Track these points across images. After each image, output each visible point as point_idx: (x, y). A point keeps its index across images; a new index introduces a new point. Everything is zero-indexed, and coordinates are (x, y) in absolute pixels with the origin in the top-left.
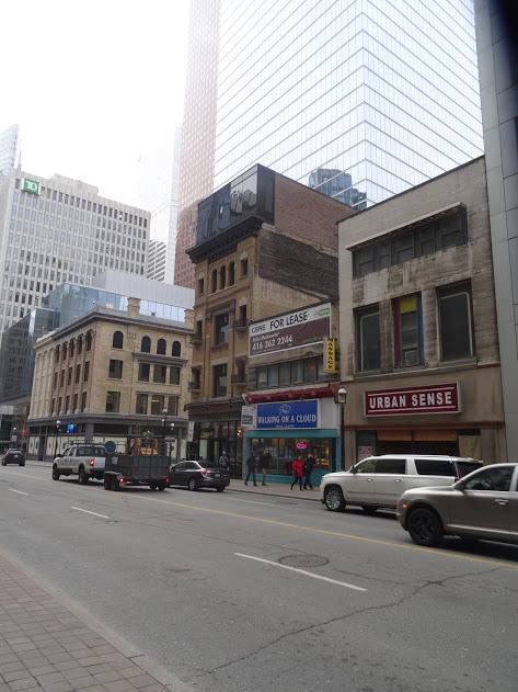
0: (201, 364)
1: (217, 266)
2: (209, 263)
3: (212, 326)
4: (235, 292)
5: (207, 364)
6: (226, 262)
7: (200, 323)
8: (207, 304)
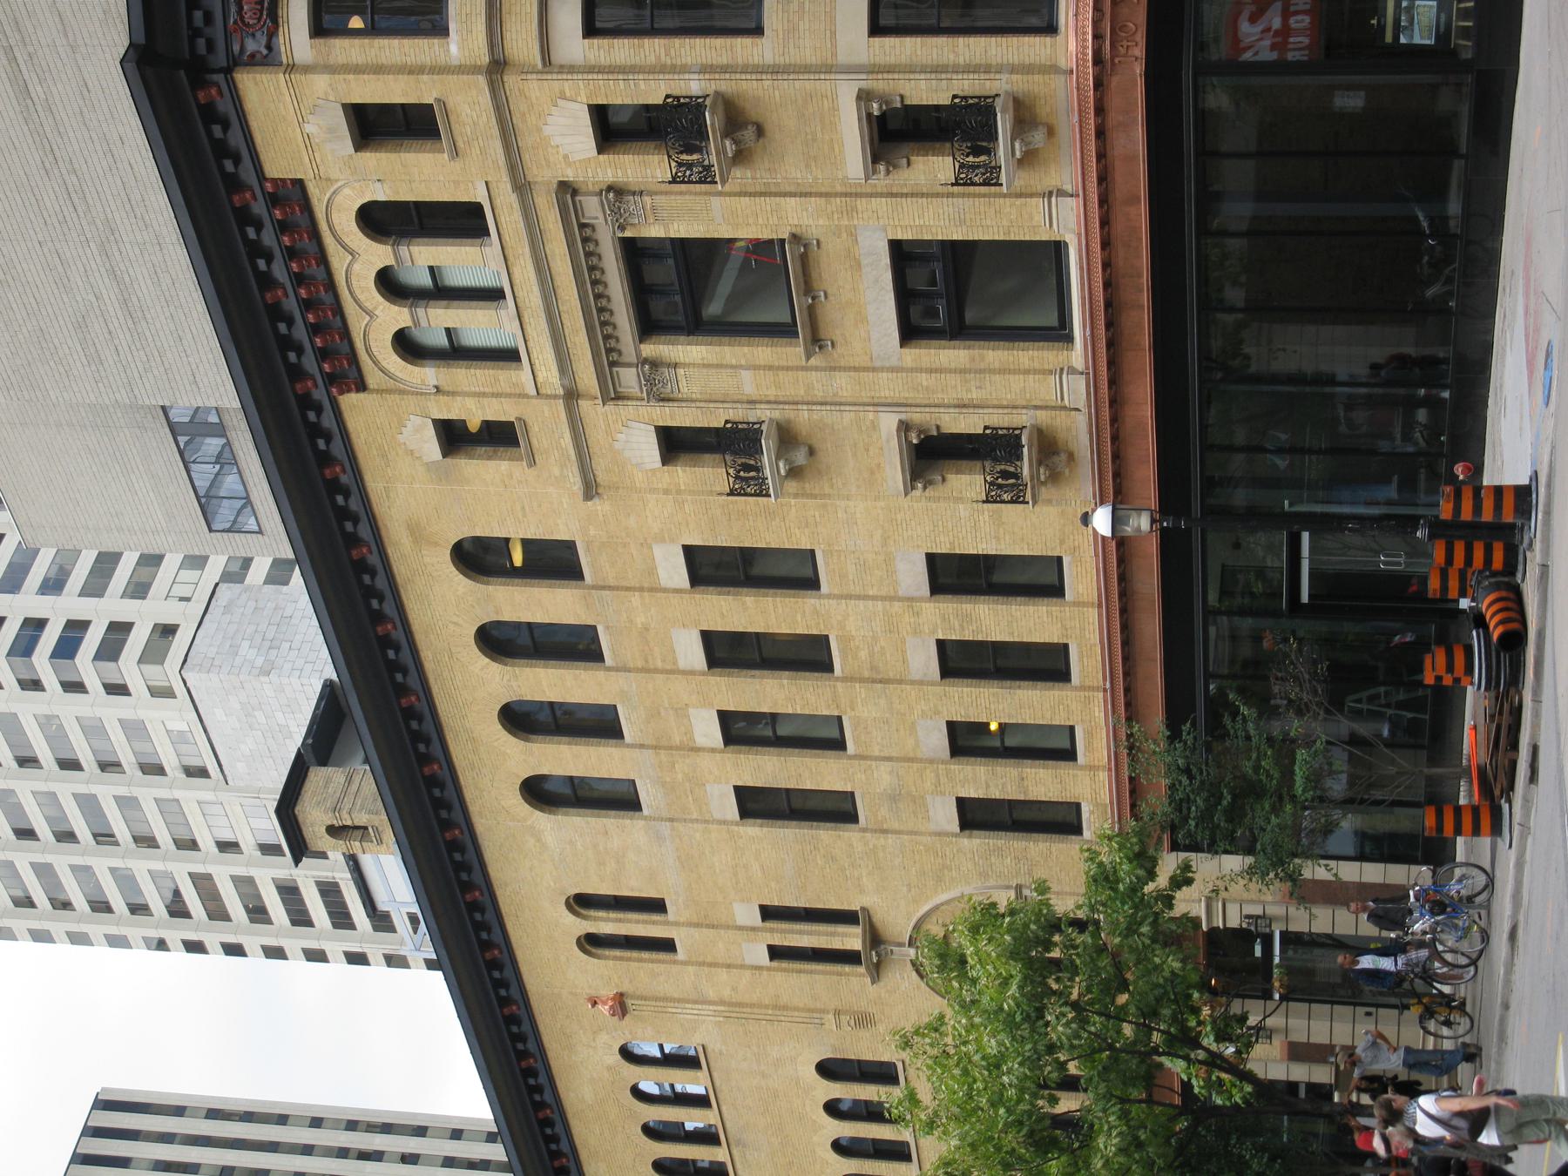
0: (889, 422)
1: (375, 322)
2: (362, 386)
3: (689, 355)
4: (522, 187)
5: (888, 386)
6: (358, 261)
7: (676, 444)
8: (572, 396)
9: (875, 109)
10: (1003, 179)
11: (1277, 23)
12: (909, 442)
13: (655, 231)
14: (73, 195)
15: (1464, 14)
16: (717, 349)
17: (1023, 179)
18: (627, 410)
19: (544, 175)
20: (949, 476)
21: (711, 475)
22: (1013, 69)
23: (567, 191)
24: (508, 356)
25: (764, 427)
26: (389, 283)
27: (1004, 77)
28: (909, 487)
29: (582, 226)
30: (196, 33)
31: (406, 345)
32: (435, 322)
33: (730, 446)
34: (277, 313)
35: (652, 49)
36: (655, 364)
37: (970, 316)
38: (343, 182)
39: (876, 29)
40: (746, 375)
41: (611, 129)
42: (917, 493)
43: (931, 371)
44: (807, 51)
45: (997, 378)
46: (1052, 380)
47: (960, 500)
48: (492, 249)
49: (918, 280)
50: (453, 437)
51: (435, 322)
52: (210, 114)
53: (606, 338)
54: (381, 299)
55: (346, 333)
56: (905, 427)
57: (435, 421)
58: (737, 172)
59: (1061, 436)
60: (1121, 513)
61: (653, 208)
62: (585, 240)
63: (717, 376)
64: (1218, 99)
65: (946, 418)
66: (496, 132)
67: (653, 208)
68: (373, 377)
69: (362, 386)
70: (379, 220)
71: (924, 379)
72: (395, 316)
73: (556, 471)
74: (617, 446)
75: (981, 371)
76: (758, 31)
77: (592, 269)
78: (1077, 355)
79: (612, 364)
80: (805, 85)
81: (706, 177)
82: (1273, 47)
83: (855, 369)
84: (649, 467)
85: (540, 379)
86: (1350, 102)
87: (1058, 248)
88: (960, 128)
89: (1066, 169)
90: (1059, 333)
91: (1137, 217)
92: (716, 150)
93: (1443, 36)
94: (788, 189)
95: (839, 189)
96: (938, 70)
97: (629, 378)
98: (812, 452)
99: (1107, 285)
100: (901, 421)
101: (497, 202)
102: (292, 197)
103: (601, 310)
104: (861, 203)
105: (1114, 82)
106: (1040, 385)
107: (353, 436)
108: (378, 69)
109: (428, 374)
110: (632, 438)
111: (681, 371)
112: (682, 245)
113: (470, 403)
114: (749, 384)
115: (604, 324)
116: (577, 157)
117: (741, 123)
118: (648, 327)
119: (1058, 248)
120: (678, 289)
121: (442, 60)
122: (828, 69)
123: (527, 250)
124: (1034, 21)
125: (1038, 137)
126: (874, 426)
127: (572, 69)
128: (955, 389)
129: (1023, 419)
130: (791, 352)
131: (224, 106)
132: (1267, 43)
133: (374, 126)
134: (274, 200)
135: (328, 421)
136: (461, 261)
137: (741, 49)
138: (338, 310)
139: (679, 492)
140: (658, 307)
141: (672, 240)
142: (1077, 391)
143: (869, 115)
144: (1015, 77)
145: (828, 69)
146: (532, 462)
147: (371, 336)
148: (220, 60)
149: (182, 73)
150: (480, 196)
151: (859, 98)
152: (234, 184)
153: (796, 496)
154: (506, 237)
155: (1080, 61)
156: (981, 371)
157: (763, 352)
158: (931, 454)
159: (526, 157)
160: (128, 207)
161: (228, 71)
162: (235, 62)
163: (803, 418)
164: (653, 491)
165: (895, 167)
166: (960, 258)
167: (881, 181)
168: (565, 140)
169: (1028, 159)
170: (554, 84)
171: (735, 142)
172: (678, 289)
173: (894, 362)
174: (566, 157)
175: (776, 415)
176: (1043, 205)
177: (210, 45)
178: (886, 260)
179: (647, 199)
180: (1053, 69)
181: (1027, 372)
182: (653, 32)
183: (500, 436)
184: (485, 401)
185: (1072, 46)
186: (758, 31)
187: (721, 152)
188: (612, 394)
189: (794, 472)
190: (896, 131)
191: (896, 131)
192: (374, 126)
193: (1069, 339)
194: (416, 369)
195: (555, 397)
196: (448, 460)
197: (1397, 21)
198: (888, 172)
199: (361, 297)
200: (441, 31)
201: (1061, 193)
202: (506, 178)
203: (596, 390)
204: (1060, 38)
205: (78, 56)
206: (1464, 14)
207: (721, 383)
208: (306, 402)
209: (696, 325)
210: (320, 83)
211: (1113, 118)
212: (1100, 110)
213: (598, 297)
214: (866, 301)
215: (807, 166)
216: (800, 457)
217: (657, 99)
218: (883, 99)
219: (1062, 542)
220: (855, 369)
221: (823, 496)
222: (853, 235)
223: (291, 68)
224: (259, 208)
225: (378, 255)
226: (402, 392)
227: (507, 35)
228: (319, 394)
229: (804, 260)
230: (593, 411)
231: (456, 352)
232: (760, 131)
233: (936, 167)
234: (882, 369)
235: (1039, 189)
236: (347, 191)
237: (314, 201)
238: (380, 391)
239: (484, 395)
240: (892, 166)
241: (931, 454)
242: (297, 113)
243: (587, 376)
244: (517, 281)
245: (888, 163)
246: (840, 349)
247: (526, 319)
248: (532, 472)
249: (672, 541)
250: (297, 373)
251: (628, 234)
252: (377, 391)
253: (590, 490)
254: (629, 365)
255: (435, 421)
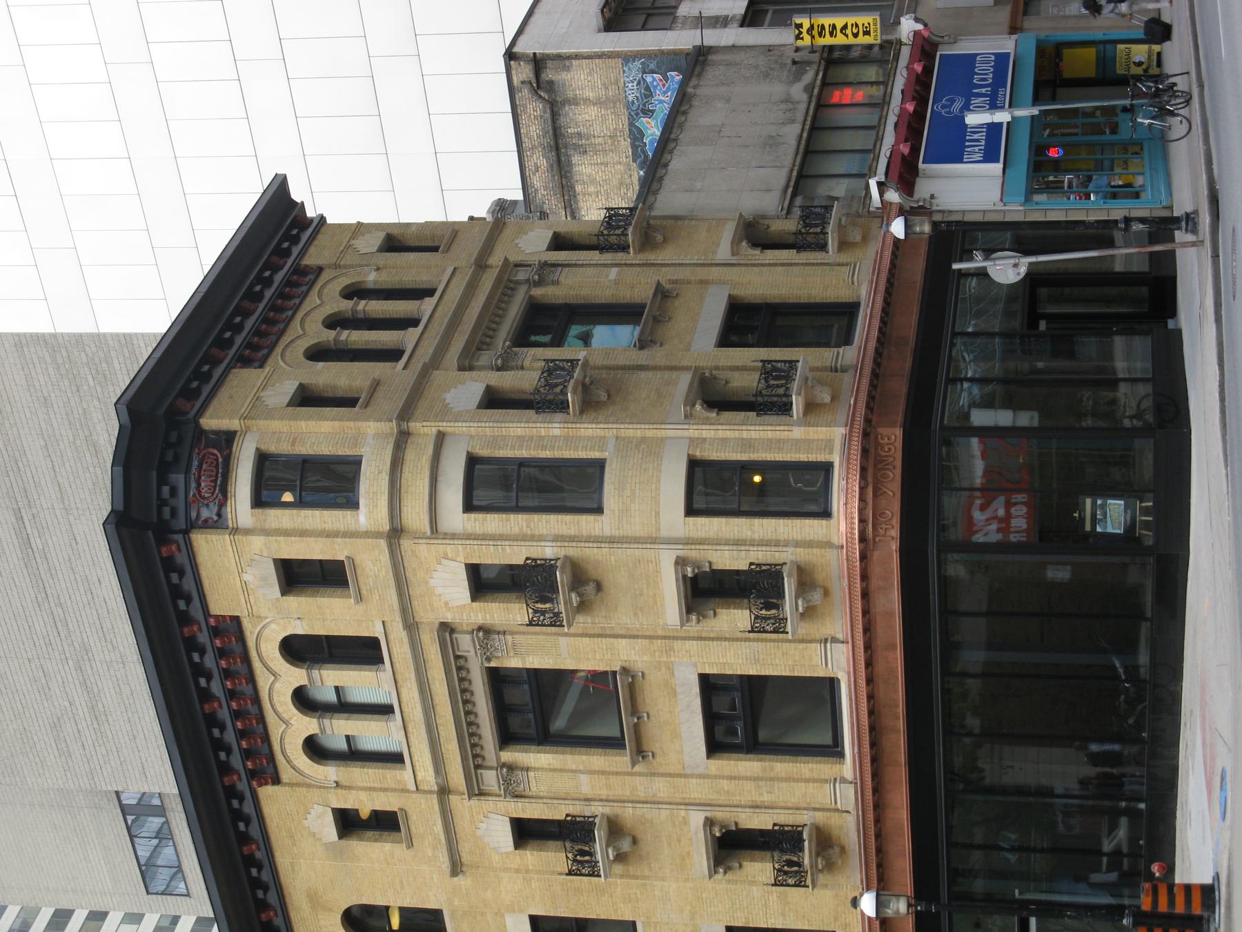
0: (697, 819)
1: (290, 729)
2: (276, 780)
4: (411, 626)
5: (697, 790)
6: (278, 680)
7: (526, 832)
8: (444, 792)
9: (689, 572)
10: (789, 628)
11: (1001, 512)
12: (713, 836)
13: (514, 663)
14: (59, 624)
15: (1145, 511)
16: (561, 757)
17: (805, 629)
18: (487, 804)
19: (429, 616)
20: (745, 864)
21: (554, 858)
22: (797, 544)
23: (446, 630)
24: (394, 758)
25: (597, 821)
26: (302, 699)
27: (790, 549)
28: (713, 872)
29: (457, 657)
30: (163, 503)
31: (315, 749)
32: (338, 730)
33: (569, 835)
34: (212, 721)
35: (517, 522)
36: (511, 768)
37: (763, 735)
38: (271, 618)
39: (691, 511)
40: (584, 778)
41: (483, 583)
42: (719, 876)
43: (731, 778)
44: (637, 527)
45: (784, 784)
46: (828, 788)
47: (753, 883)
48: (385, 674)
49: (721, 706)
50: (348, 822)
51: (338, 730)
52: (170, 565)
53: (473, 746)
54: (295, 711)
55: (266, 738)
56: (710, 823)
57: (333, 810)
58: (580, 618)
59: (835, 833)
60: (883, 898)
61: (514, 645)
62: (459, 669)
63: (560, 778)
64: (956, 569)
65: (743, 816)
66: (392, 583)
67: (514, 645)
68: (286, 774)
69: (276, 780)
70: (299, 649)
71: (725, 784)
72: (306, 725)
73: (429, 852)
74: (479, 833)
75: (772, 779)
76: (599, 510)
77: (464, 691)
78: (847, 768)
79: (477, 767)
80: (635, 552)
81: (556, 621)
82: (999, 530)
83: (670, 775)
84: (503, 850)
85: (419, 778)
86: (1059, 573)
87: (832, 683)
88: (756, 588)
89: (838, 622)
90: (833, 750)
91: (894, 660)
92: (564, 600)
93: (1130, 528)
94: (620, 632)
95: (660, 633)
96: (738, 543)
97: (490, 778)
98: (635, 841)
99: (871, 713)
100: (707, 819)
101: (391, 637)
102: (231, 631)
103: (470, 724)
104: (677, 644)
105: (876, 555)
106: (818, 790)
107: (268, 820)
108: (303, 533)
109: (330, 772)
110: (490, 827)
111: (531, 774)
112: (536, 675)
113: (363, 796)
114: (586, 785)
115: (471, 735)
116: (453, 604)
117: (586, 584)
118: (507, 738)
119: (832, 683)
120: (531, 709)
121: (353, 528)
122: (654, 540)
123: (413, 675)
124: (813, 508)
125: (816, 597)
126: (685, 822)
127: (454, 536)
128: (749, 793)
129: (804, 818)
130: (620, 760)
131: (181, 559)
132: (994, 527)
133: (296, 576)
134: (216, 632)
135: (248, 808)
136: (361, 683)
137: (585, 524)
138: (261, 719)
139: (527, 871)
140: (515, 722)
141: (528, 670)
142: (847, 796)
143: (685, 577)
144: (798, 550)
145: (654, 540)
146: (410, 845)
147: (287, 740)
148: (181, 523)
149: (150, 533)
150: (378, 632)
151: (677, 563)
152: (185, 619)
153: (622, 876)
154: (397, 665)
155: (849, 538)
156: (772, 779)
157: (597, 760)
158: (730, 845)
159: (415, 603)
160: (101, 634)
161: (186, 532)
162: (192, 526)
163: (628, 813)
164: (506, 870)
165: (704, 617)
166: (754, 687)
167: (693, 627)
168: (446, 591)
169: (809, 613)
170: (440, 547)
171: (580, 595)
172: (531, 709)
173: (701, 770)
174: (446, 604)
175: (607, 810)
176: (822, 648)
177: (174, 512)
178: (696, 689)
179: (509, 638)
180: (828, 544)
181: (807, 781)
182: (518, 509)
183: (385, 823)
184: (375, 794)
185: (843, 527)
186: (599, 510)
187: (568, 602)
188: (476, 791)
189: (621, 858)
190: (705, 589)
191: (705, 589)
192: (296, 576)
193: (841, 755)
194: (321, 767)
195: (431, 792)
196: (343, 842)
197: (1094, 515)
198: (698, 621)
199: (280, 709)
200: (354, 505)
201: (835, 640)
202: (398, 619)
203: (463, 788)
204: (833, 521)
205: (71, 518)
206: (1145, 511)
207: (563, 784)
208: (232, 792)
209: (545, 738)
210: (257, 542)
211: (875, 582)
212: (864, 577)
213: (467, 713)
214: (680, 722)
215: (636, 614)
216: (625, 845)
217: (519, 561)
218: (696, 564)
219: (836, 919)
220: (670, 775)
221: (644, 877)
222: (670, 669)
223: (235, 531)
224: (203, 638)
225: (295, 676)
226: (309, 786)
227: (404, 509)
228: (242, 786)
229: (632, 689)
230: (461, 805)
231: (354, 755)
232: (599, 587)
233: (736, 618)
234: (692, 776)
235: (818, 637)
236: (273, 626)
237: (247, 633)
238: (291, 785)
239: (374, 789)
240: (702, 616)
241: (730, 845)
242: (237, 565)
243: (456, 776)
244: (404, 700)
245: (699, 614)
246: (659, 759)
247: (410, 729)
248: (410, 852)
249: (521, 911)
250: (225, 769)
251: (493, 664)
252: (291, 785)
253: (456, 868)
254: (491, 768)
255: (333, 810)
